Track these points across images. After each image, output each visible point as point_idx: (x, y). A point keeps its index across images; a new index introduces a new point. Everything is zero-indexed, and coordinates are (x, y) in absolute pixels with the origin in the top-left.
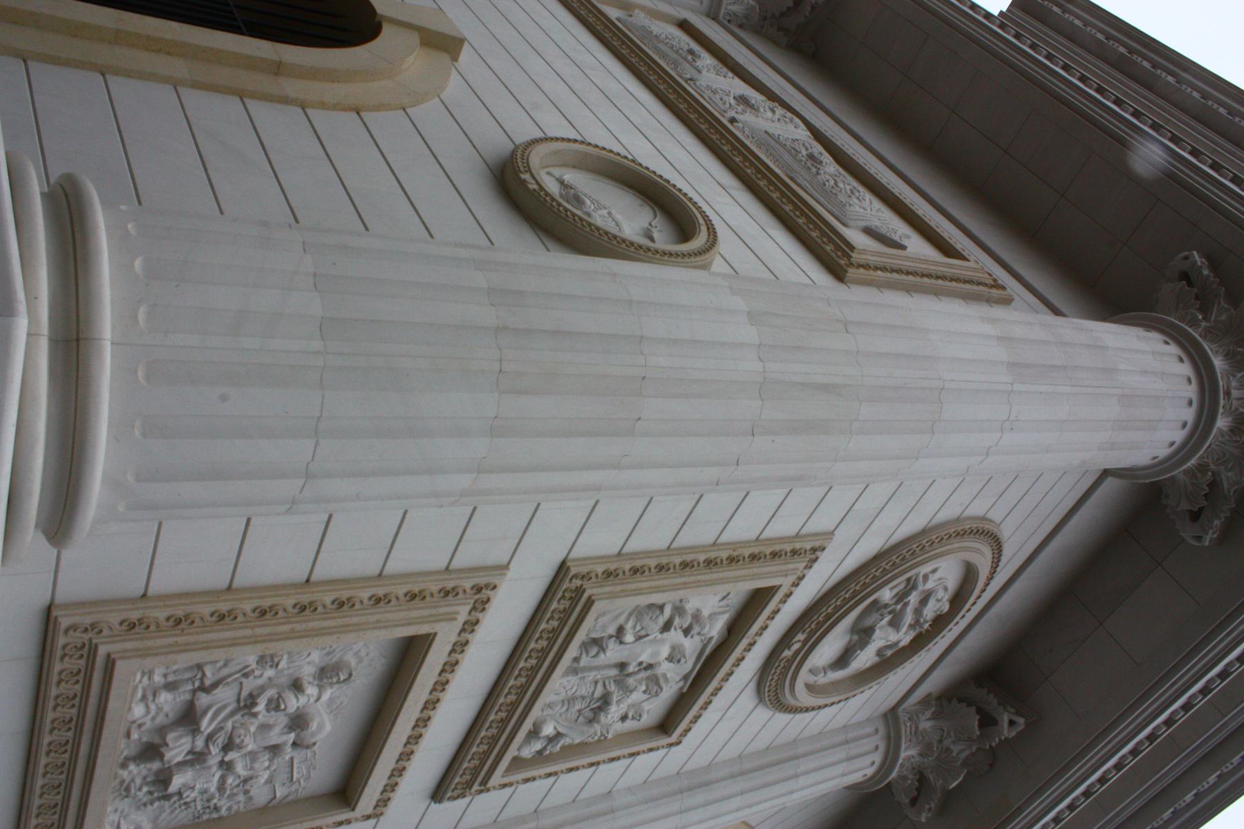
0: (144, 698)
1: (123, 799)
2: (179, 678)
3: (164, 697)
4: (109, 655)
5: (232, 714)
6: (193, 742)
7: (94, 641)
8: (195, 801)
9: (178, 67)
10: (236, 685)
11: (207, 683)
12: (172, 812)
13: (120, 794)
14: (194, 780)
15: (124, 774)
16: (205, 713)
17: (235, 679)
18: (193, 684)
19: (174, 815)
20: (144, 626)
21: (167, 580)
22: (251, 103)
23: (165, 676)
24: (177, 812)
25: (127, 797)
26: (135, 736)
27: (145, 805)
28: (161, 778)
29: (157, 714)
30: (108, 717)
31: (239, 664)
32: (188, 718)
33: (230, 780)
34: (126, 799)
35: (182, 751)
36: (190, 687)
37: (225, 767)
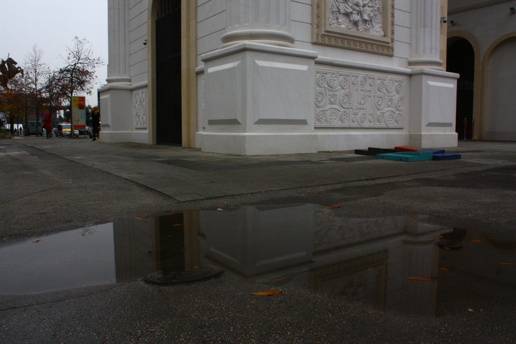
0: (340, 25)
1: (370, 31)
2: (335, 17)
3: (340, 20)
4: (325, 32)
5: (348, 4)
6: (355, 14)
7: (321, 34)
8: (375, 14)
9: (192, 23)
10: (339, 3)
11: (337, 10)
12: (377, 19)
13: (368, 31)
14: (366, 13)
15: (361, 30)
16: (346, 11)
17: (338, 3)
18: (337, 13)
19: (379, 19)
20: (318, 24)
21: (308, 20)
22: (199, 4)
23: (334, 20)
24: (377, 18)
25: (369, 30)
26: (350, 27)
27: (372, 26)
28: (365, 21)
29: (345, 22)
30: (342, 32)
31: (333, 2)
32: (347, 15)
33: (370, 5)
34: (370, 30)
35: (357, 17)
36: (338, 15)
37: (365, 6)
